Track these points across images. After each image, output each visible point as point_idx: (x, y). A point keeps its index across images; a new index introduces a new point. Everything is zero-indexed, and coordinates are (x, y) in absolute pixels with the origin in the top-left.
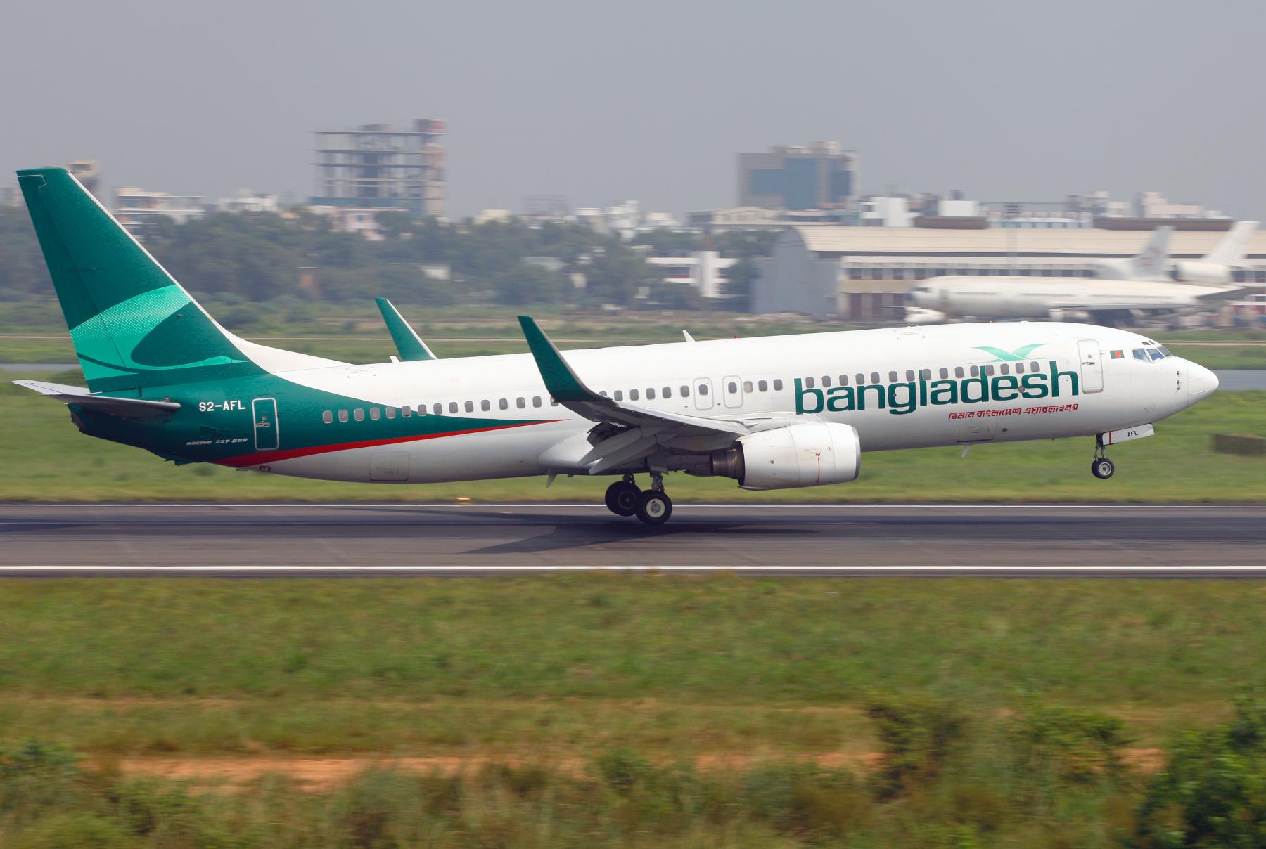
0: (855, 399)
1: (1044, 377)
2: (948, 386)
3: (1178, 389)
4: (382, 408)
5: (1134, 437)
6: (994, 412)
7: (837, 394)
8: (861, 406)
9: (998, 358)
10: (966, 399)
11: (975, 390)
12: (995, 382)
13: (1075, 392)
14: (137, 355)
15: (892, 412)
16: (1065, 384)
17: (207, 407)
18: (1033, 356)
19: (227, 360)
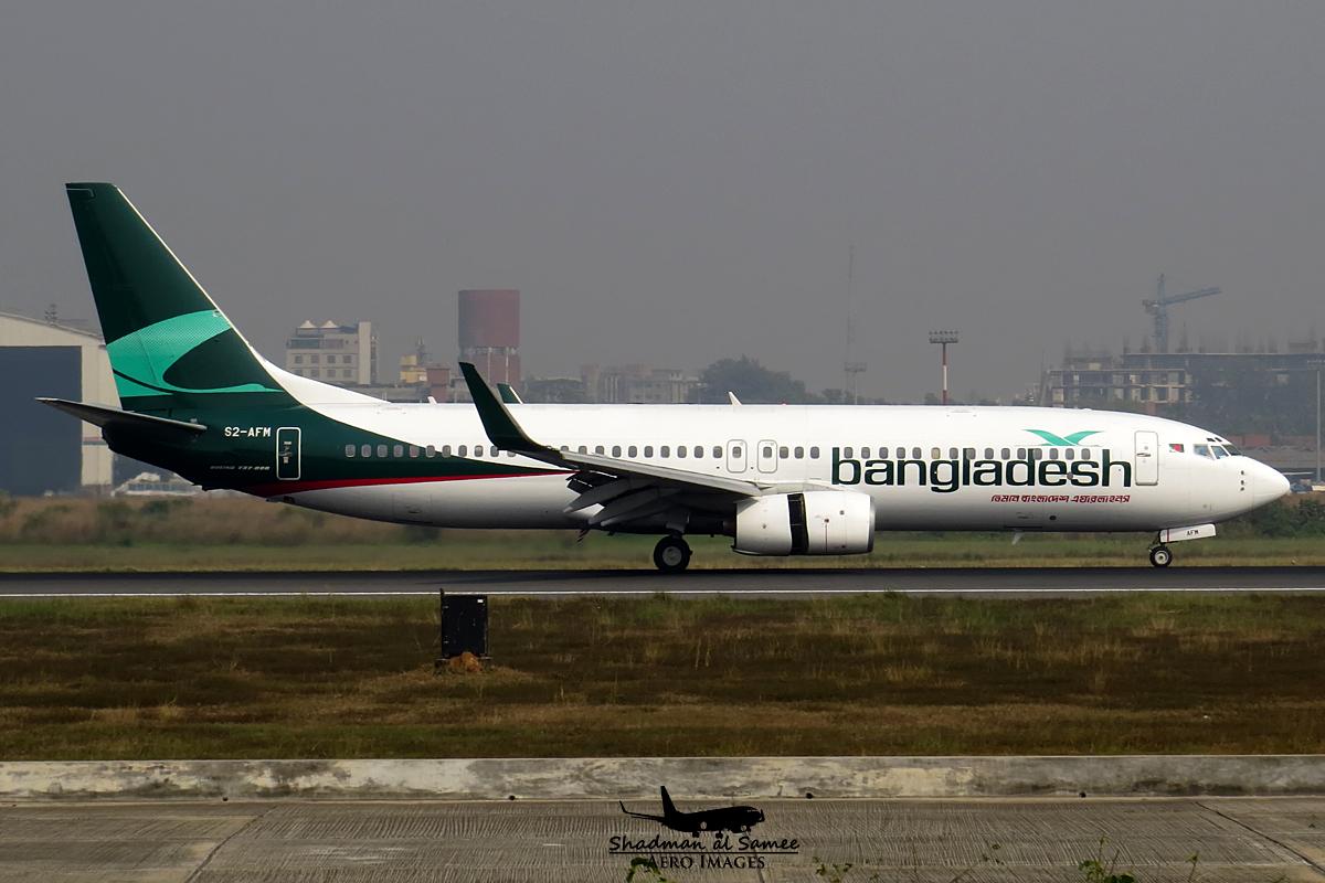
0: (895, 474)
1: (1095, 465)
2: (993, 467)
3: (1243, 489)
4: (406, 446)
5: (1194, 536)
6: (1040, 497)
7: (875, 466)
8: (901, 481)
9: (1046, 442)
10: (1011, 481)
11: (1021, 472)
12: (1043, 465)
13: (1127, 483)
14: (169, 376)
15: (934, 489)
16: (1117, 473)
17: (233, 432)
18: (1085, 442)
19: (259, 388)
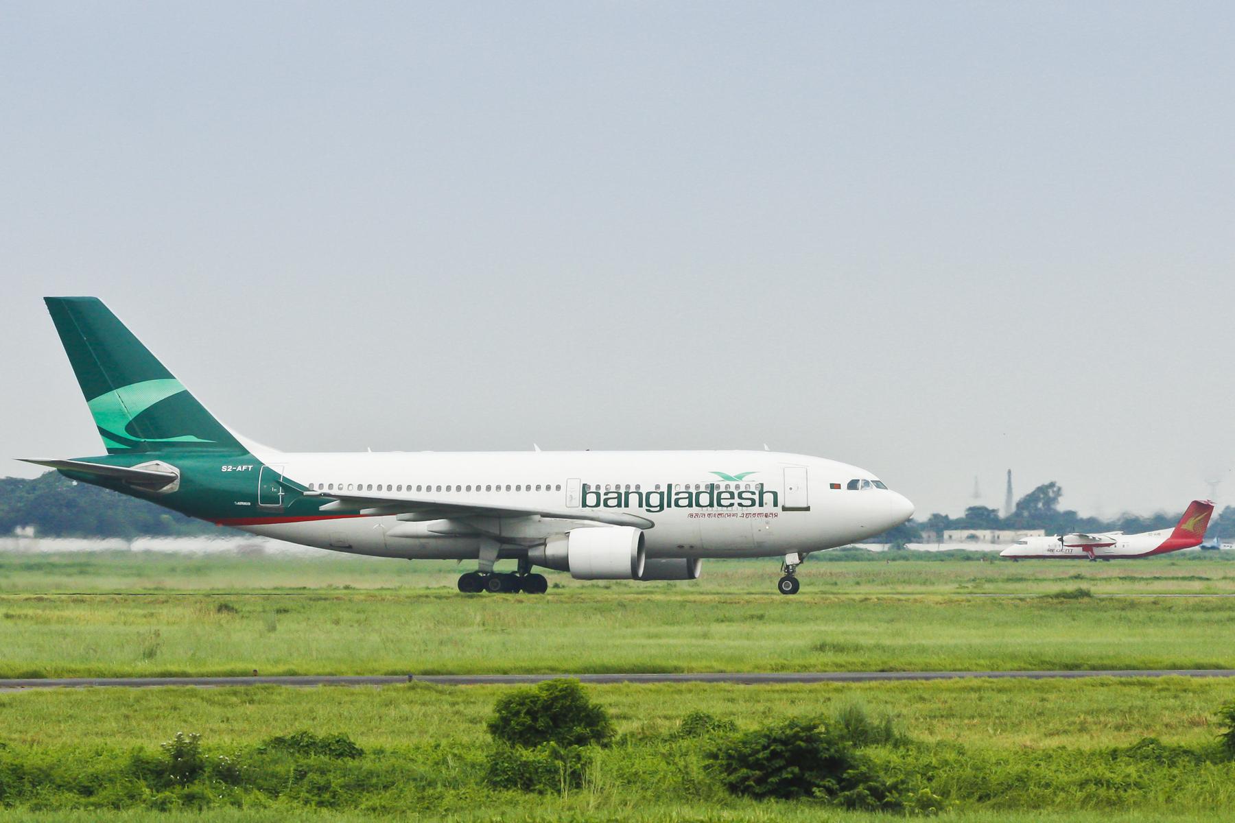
10: (698, 505)
11: (704, 499)
12: (719, 494)
15: (648, 510)
16: (768, 498)
